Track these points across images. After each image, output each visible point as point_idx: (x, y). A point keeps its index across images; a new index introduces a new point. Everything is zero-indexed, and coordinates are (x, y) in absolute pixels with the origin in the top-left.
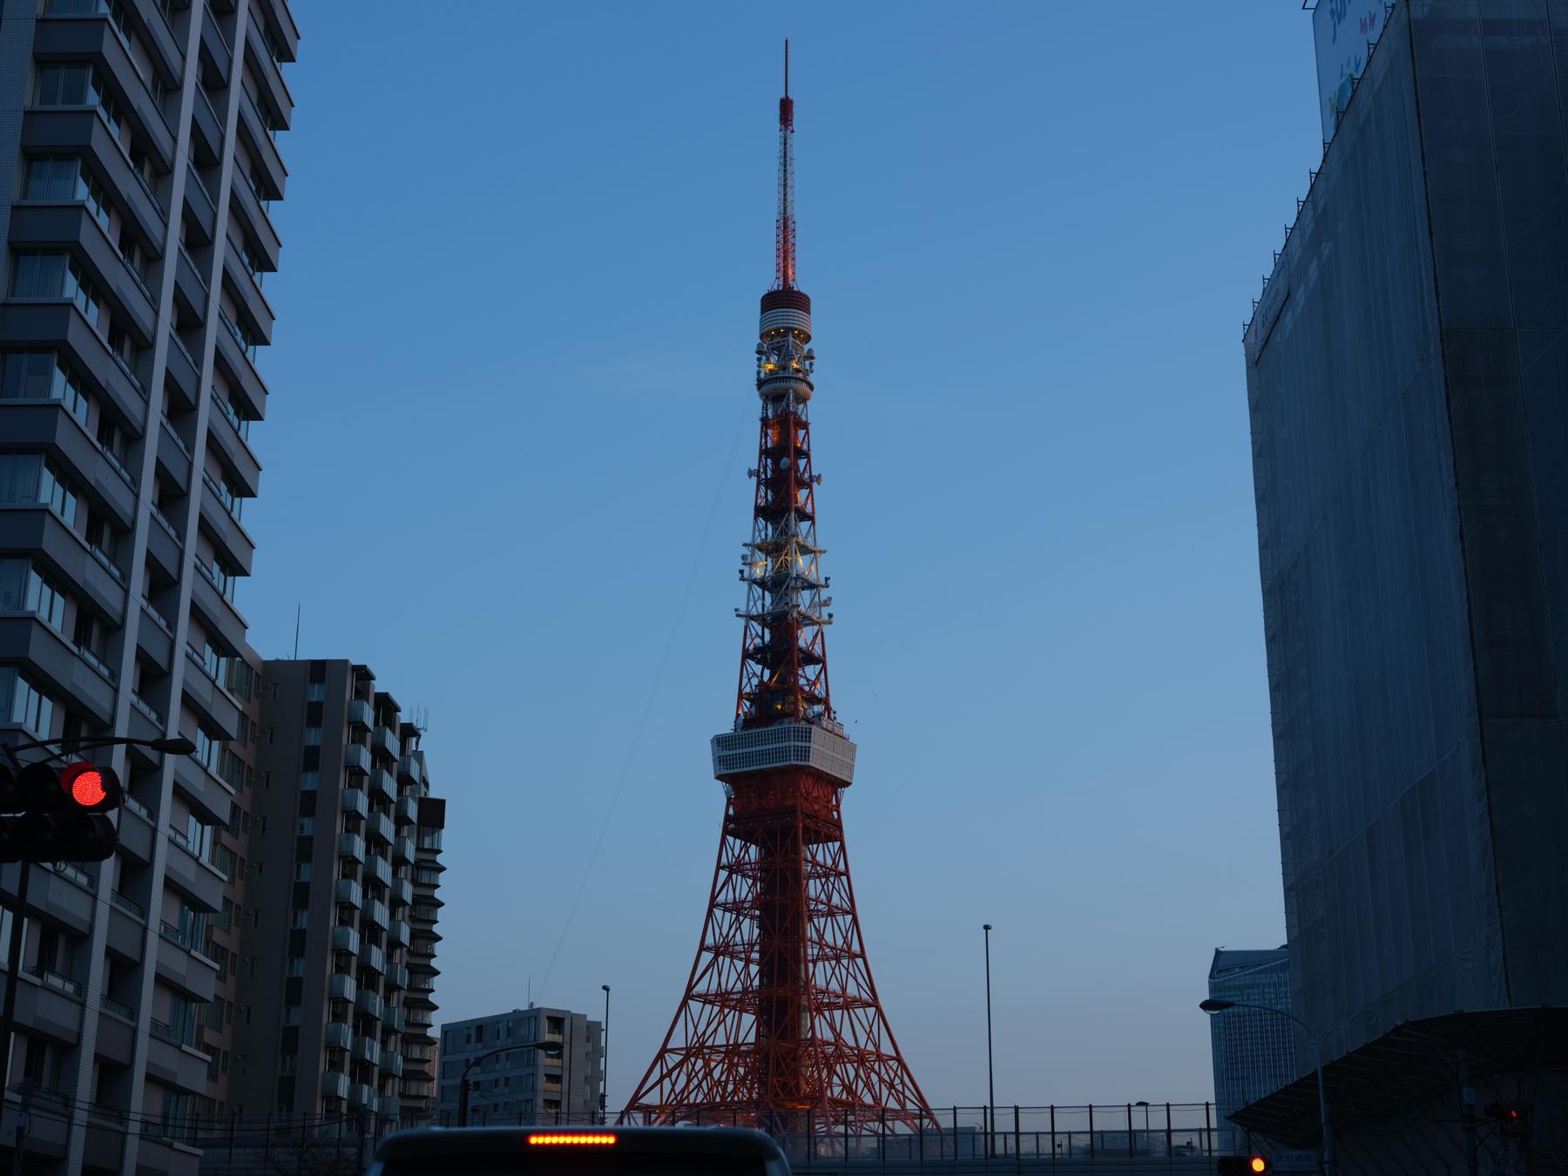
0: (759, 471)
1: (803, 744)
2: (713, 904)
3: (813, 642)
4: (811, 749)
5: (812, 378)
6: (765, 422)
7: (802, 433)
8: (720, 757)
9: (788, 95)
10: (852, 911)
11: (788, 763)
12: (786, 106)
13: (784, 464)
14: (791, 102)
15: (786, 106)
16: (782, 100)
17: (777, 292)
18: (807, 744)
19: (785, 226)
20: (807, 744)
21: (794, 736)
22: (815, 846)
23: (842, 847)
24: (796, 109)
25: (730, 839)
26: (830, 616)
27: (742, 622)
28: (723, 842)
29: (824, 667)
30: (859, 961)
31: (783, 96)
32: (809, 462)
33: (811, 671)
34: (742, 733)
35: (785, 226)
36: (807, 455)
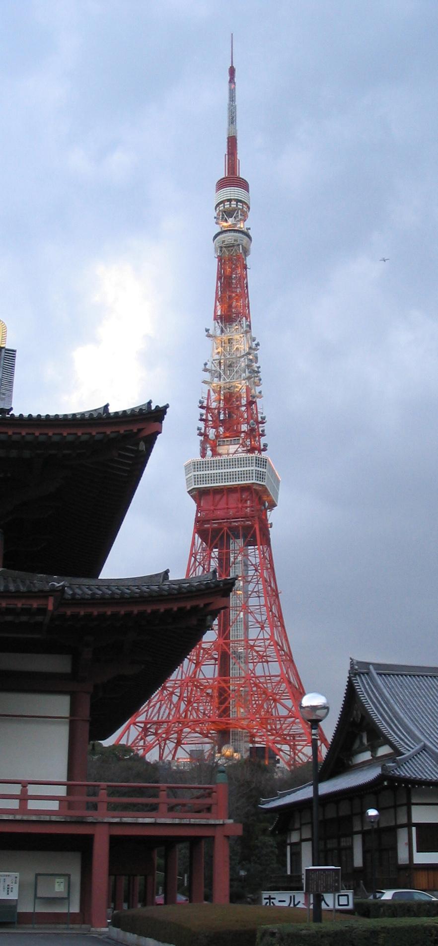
11: (251, 482)
12: (232, 71)
15: (232, 71)
16: (231, 67)
18: (264, 470)
19: (232, 142)
20: (264, 470)
21: (256, 463)
24: (237, 74)
26: (260, 392)
27: (206, 387)
34: (212, 459)
35: (232, 142)
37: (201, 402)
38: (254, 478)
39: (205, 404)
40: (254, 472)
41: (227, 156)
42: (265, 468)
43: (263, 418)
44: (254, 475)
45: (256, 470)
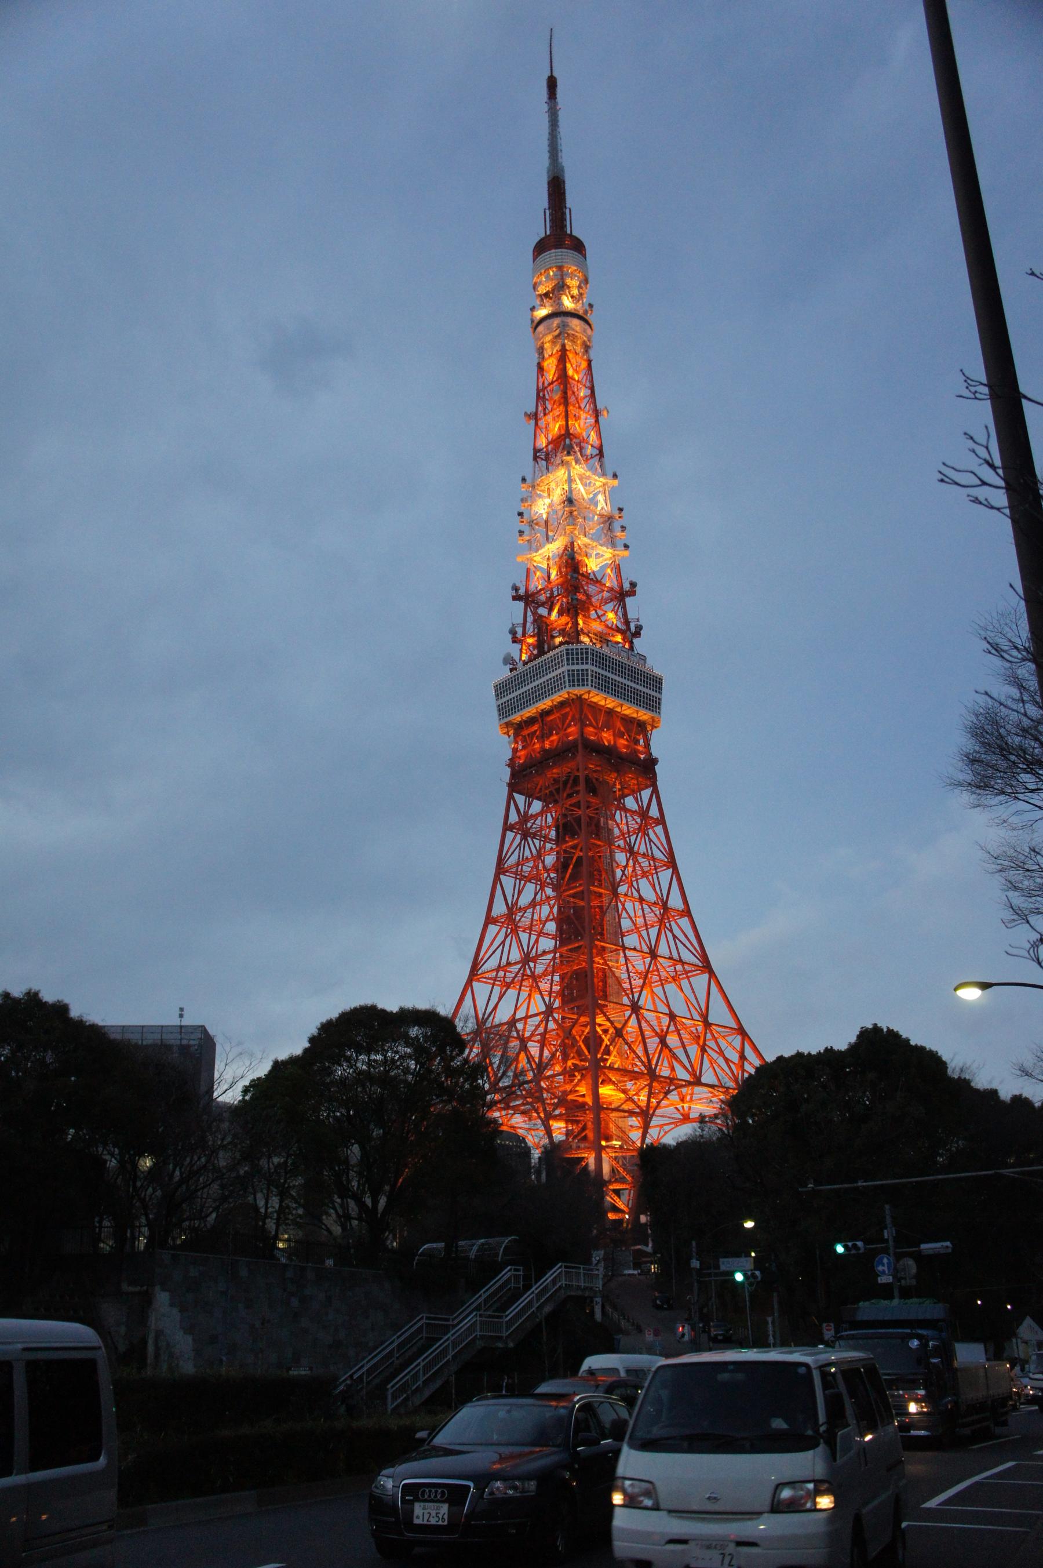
0: (536, 414)
1: (580, 667)
2: (501, 869)
4: (589, 672)
5: (589, 317)
8: (499, 705)
9: (555, 74)
12: (552, 84)
13: (557, 395)
14: (555, 79)
15: (552, 84)
16: (549, 77)
17: (542, 240)
18: (584, 667)
19: (557, 189)
20: (584, 667)
21: (568, 659)
25: (520, 799)
28: (510, 797)
30: (684, 922)
31: (548, 74)
35: (557, 189)
37: (516, 589)
38: (567, 684)
39: (522, 592)
40: (566, 673)
41: (548, 212)
42: (587, 663)
43: (633, 585)
44: (567, 679)
45: (569, 671)
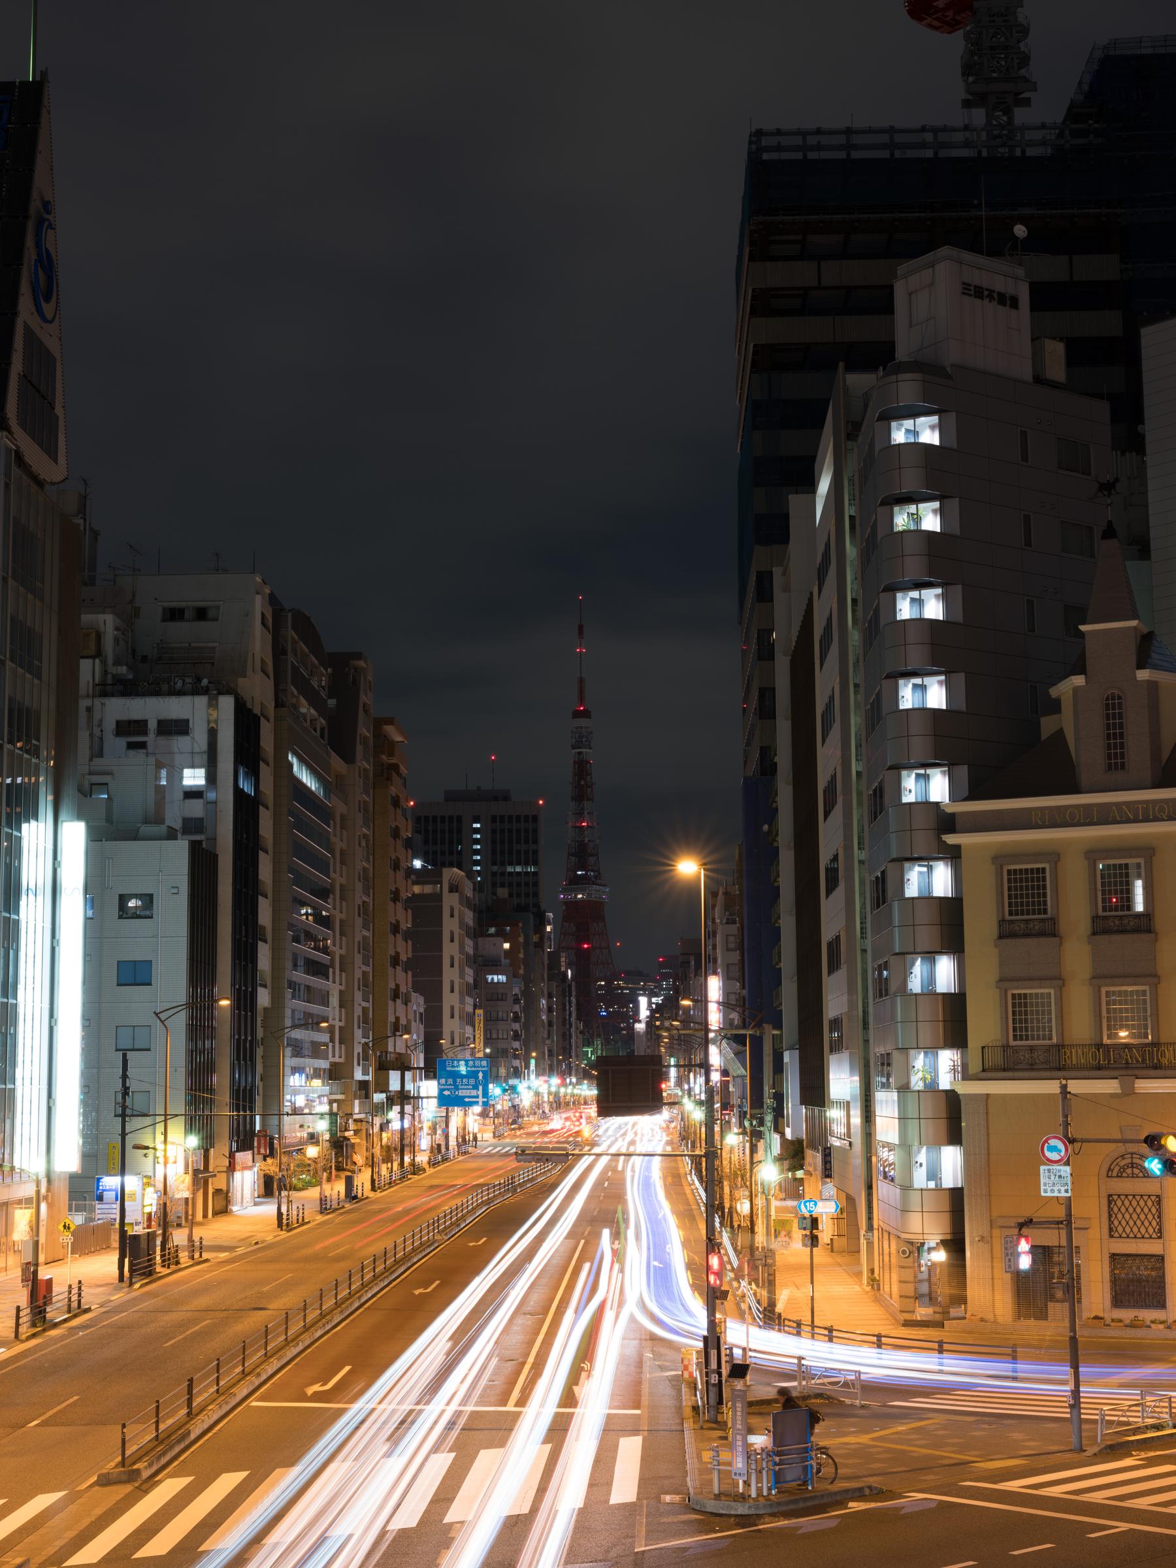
3: (594, 849)
6: (574, 762)
7: (589, 765)
10: (608, 948)
12: (581, 628)
14: (582, 626)
15: (581, 628)
19: (581, 681)
22: (595, 924)
23: (605, 925)
28: (562, 924)
29: (598, 858)
32: (591, 778)
33: (592, 860)
35: (581, 681)
36: (591, 774)
